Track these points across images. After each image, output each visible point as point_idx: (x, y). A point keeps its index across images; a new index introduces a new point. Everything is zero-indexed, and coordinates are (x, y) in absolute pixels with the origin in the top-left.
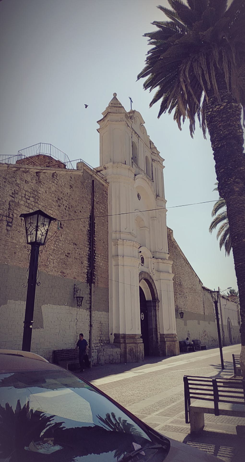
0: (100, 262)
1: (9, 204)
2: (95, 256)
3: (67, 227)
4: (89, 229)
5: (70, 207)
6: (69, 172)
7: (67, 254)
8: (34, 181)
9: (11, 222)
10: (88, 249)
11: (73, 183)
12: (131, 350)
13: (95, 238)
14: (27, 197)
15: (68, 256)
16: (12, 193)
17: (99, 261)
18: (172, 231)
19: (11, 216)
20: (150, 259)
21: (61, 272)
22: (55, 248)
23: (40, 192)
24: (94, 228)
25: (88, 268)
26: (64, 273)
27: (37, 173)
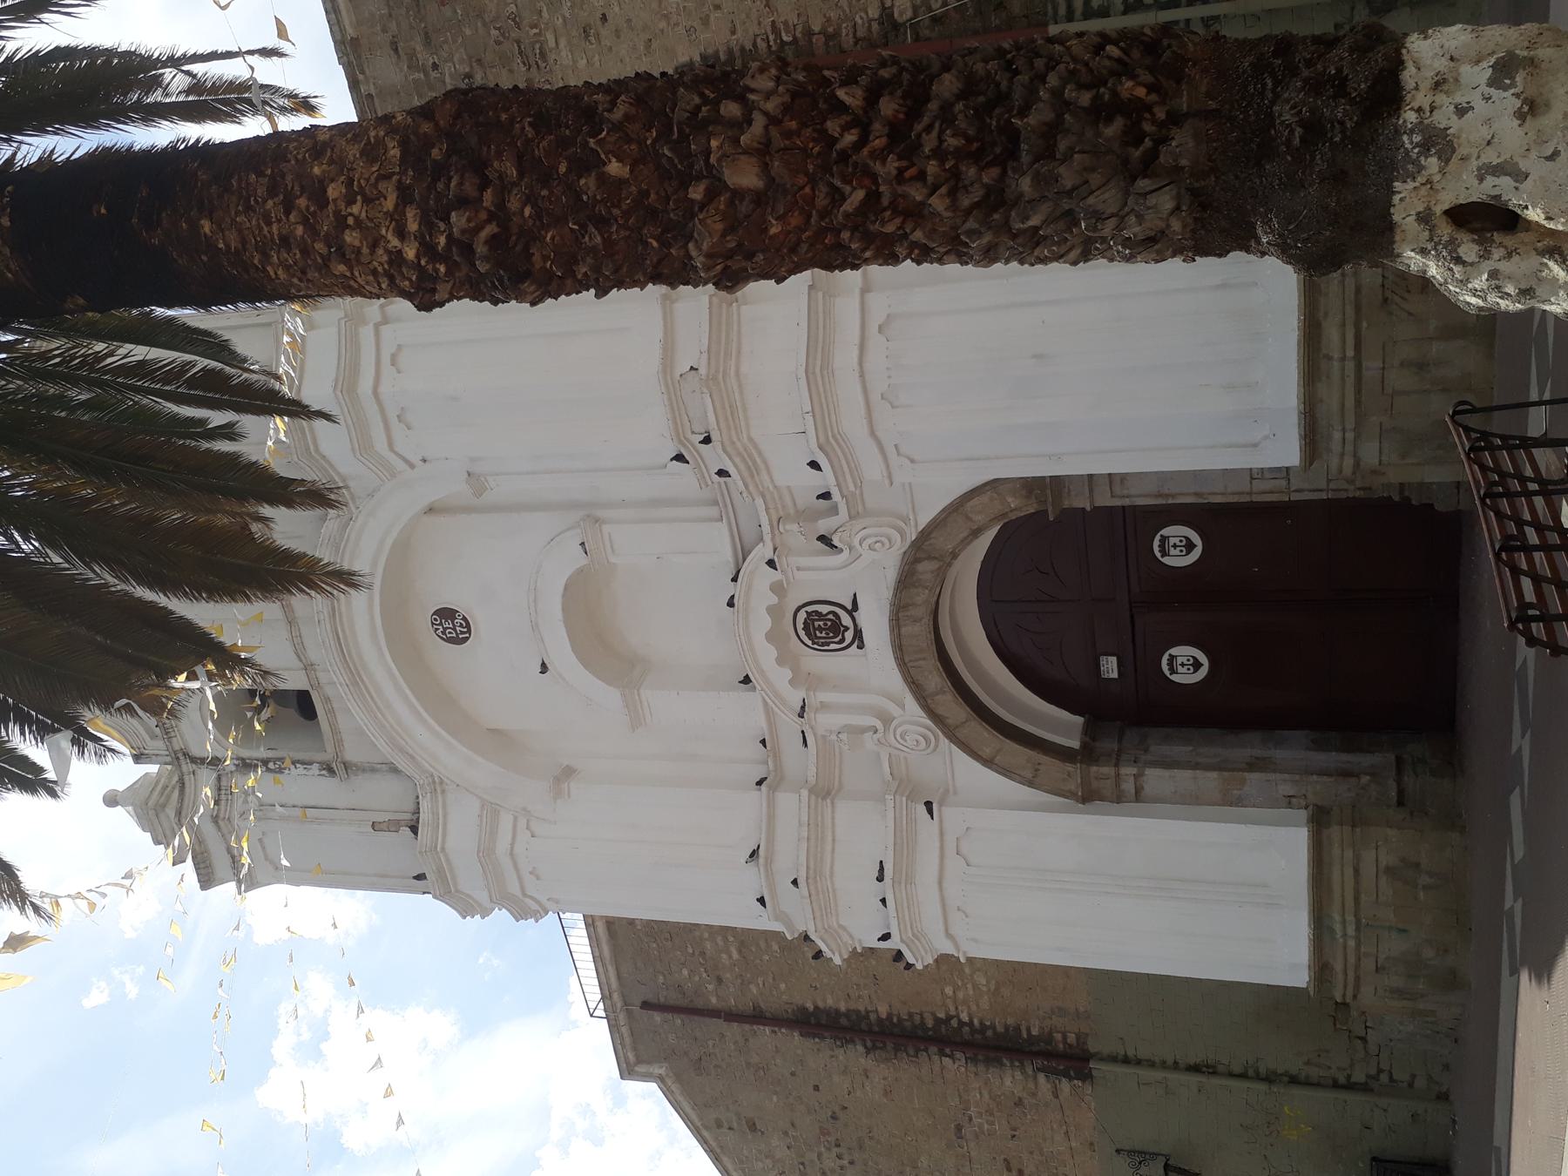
0: (975, 986)
4: (860, 1048)
10: (946, 1061)
12: (1399, 993)
13: (883, 1011)
24: (837, 1011)
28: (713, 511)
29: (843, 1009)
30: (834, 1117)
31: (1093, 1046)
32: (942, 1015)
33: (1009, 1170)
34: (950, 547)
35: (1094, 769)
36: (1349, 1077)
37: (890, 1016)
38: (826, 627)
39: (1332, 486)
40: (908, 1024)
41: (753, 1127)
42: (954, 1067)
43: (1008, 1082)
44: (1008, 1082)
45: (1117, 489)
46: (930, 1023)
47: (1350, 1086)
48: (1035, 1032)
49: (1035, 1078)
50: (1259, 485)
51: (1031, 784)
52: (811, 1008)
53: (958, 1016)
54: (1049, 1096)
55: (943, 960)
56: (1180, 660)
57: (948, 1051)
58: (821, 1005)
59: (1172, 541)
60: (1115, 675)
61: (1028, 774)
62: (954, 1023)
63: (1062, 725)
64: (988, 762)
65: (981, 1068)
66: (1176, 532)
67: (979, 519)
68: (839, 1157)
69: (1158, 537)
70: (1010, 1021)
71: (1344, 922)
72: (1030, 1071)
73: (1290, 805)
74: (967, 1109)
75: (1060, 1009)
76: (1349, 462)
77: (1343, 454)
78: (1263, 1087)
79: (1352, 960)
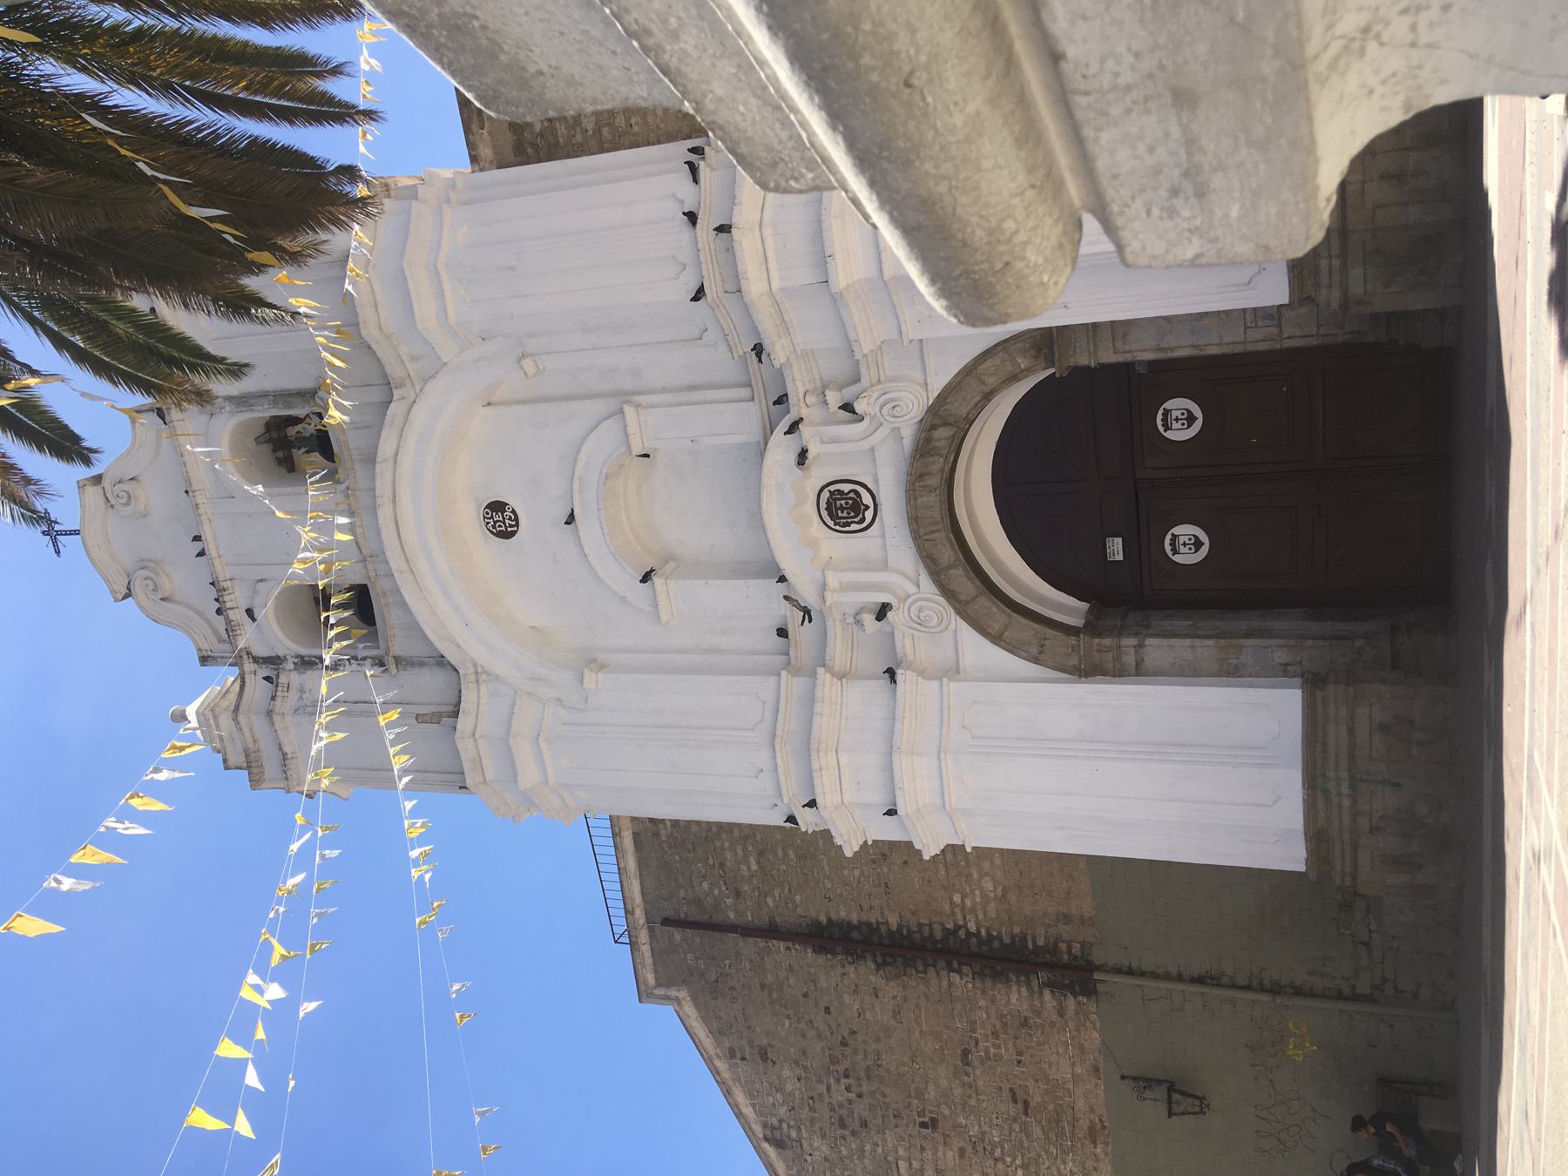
0: (984, 895)
3: (920, 1095)
4: (872, 966)
5: (841, 1068)
6: (726, 1075)
7: (1020, 1106)
10: (955, 977)
11: (744, 1043)
13: (893, 921)
15: (1026, 1103)
17: (978, 908)
21: (1094, 1142)
22: (1018, 1162)
24: (849, 924)
25: (1035, 983)
26: (1092, 1128)
28: (744, 392)
29: (855, 922)
30: (844, 1044)
31: (1097, 956)
32: (950, 926)
33: (1015, 1101)
34: (963, 412)
35: (1097, 641)
36: (1354, 987)
37: (900, 926)
39: (1322, 331)
40: (917, 936)
41: (764, 1056)
42: (961, 983)
43: (1014, 998)
44: (1014, 998)
45: (1119, 344)
46: (938, 935)
47: (1355, 998)
48: (1041, 943)
49: (1041, 994)
50: (1253, 335)
51: (1036, 661)
52: (823, 919)
53: (965, 926)
54: (1055, 1017)
55: (953, 851)
56: (1182, 539)
57: (955, 964)
58: (834, 918)
59: (1175, 414)
60: (1120, 557)
61: (1034, 650)
62: (962, 934)
63: (1067, 607)
64: (996, 639)
65: (989, 982)
66: (1178, 405)
67: (991, 381)
68: (848, 1089)
69: (1161, 411)
70: (1017, 930)
71: (1338, 778)
72: (1035, 983)
73: (1286, 674)
74: (973, 1030)
75: (1066, 916)
76: (1336, 294)
77: (1330, 286)
78: (1265, 998)
79: (1346, 820)
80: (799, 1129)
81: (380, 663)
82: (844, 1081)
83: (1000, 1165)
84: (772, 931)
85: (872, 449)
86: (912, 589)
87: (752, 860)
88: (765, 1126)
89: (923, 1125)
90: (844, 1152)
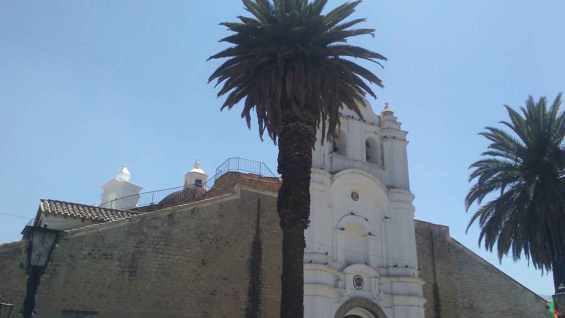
1: (133, 255)
2: (261, 288)
4: (250, 257)
5: (219, 239)
7: (212, 292)
8: (166, 225)
9: (135, 272)
10: (248, 281)
13: (263, 267)
14: (156, 243)
15: (213, 294)
16: (137, 244)
18: (448, 227)
19: (135, 265)
20: (373, 280)
21: (202, 313)
22: (194, 288)
23: (174, 233)
25: (248, 304)
27: (169, 215)
32: (262, 283)
33: (214, 291)
37: (261, 269)
38: (358, 282)
41: (221, 216)
43: (244, 297)
48: (260, 307)
52: (262, 247)
58: (263, 250)
62: (260, 286)
65: (248, 290)
68: (212, 239)
70: (262, 301)
80: (198, 219)
81: (331, 153)
82: (215, 239)
83: (192, 282)
84: (258, 231)
85: (371, 291)
86: (346, 294)
87: (275, 231)
88: (199, 209)
89: (203, 261)
90: (192, 232)
